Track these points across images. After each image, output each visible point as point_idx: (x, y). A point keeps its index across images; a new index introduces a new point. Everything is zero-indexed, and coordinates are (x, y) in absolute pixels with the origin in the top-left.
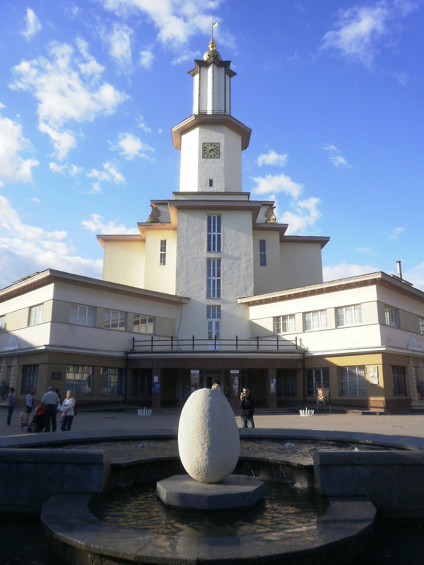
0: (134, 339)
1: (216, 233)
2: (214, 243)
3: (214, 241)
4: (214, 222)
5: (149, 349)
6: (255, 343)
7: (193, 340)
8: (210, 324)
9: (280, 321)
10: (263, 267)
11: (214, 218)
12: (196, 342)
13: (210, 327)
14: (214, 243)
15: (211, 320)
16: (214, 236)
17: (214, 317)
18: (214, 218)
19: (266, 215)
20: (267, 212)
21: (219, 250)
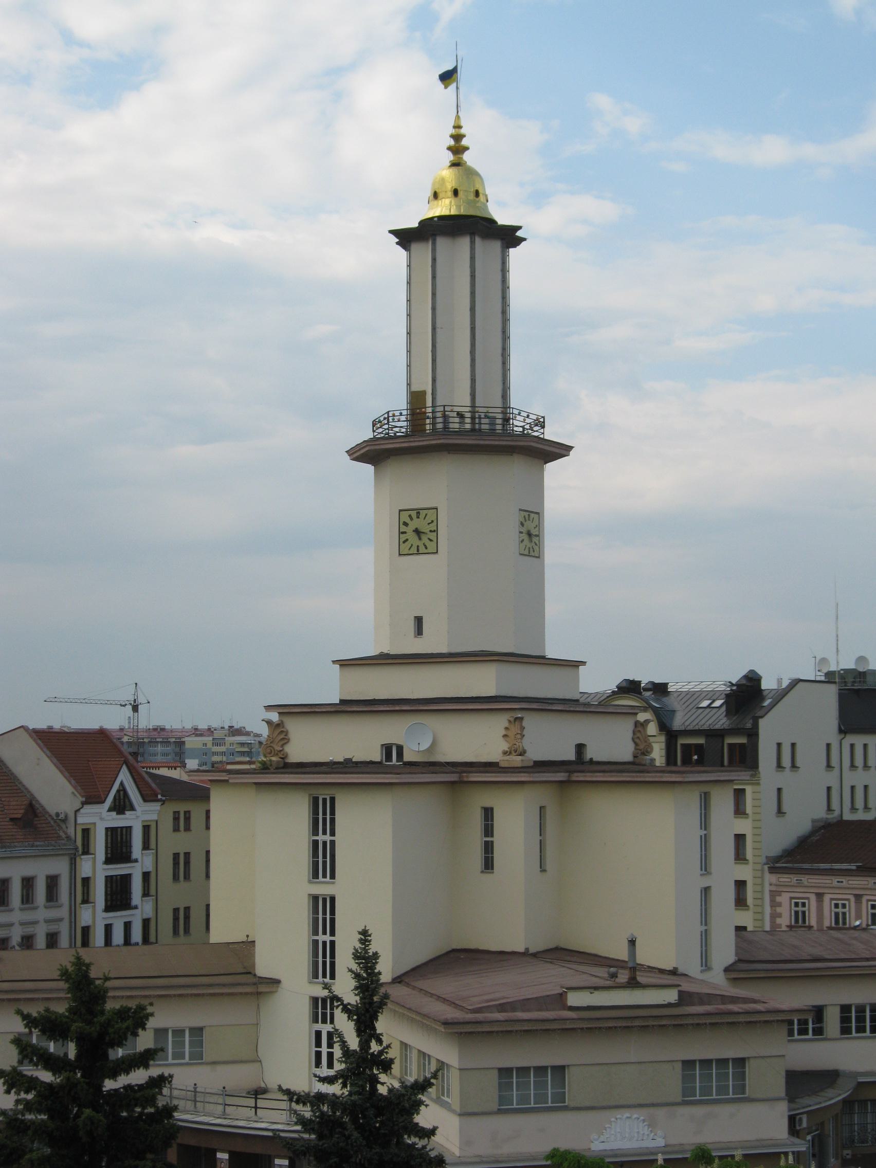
2: (323, 861)
4: (324, 813)
8: (318, 1034)
10: (487, 877)
11: (324, 800)
13: (318, 1044)
14: (323, 861)
15: (319, 1026)
17: (324, 1021)
18: (324, 800)
19: (505, 736)
20: (506, 728)
21: (333, 876)
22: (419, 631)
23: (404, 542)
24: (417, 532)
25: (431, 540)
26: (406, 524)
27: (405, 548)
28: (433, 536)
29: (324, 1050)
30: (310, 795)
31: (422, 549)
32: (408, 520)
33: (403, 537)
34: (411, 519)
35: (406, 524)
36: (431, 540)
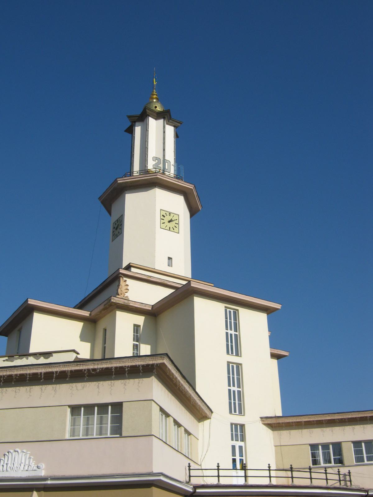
0: (189, 466)
1: (233, 332)
3: (232, 342)
5: (214, 481)
6: (307, 475)
7: (218, 469)
8: (233, 447)
9: (329, 449)
12: (222, 473)
15: (234, 443)
16: (231, 335)
17: (237, 440)
22: (170, 265)
23: (163, 223)
24: (169, 222)
25: (176, 227)
26: (163, 216)
27: (163, 226)
28: (177, 225)
29: (238, 458)
30: (226, 307)
31: (171, 229)
32: (165, 215)
33: (163, 221)
34: (167, 215)
35: (163, 216)
36: (176, 227)
